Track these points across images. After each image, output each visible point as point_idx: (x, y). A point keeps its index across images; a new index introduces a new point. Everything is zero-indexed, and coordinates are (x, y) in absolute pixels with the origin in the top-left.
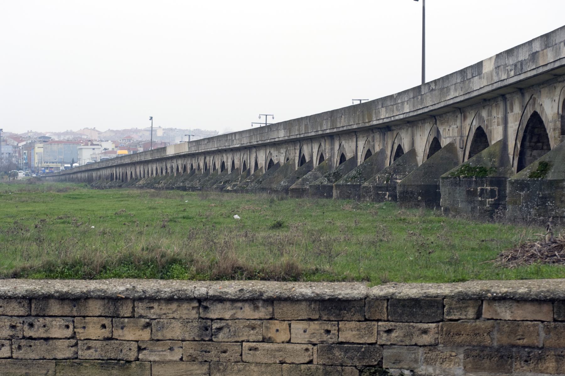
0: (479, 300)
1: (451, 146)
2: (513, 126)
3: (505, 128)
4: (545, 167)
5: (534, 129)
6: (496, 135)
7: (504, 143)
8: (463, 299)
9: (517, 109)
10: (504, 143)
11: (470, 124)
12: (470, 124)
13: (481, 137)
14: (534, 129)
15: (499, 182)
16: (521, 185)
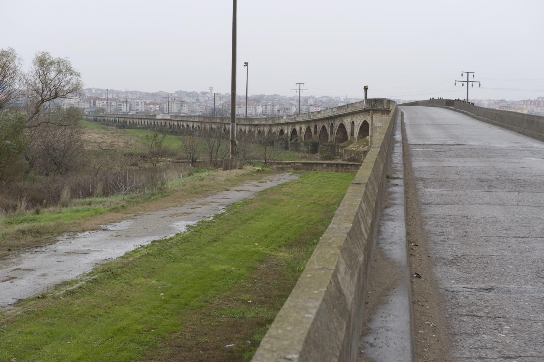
0: (295, 163)
1: (274, 132)
2: (290, 130)
3: (288, 131)
4: (297, 140)
5: (294, 132)
6: (286, 132)
7: (288, 133)
8: (293, 163)
9: (291, 127)
10: (288, 133)
11: (279, 128)
12: (279, 128)
13: (282, 132)
14: (294, 132)
15: (287, 142)
16: (292, 143)
